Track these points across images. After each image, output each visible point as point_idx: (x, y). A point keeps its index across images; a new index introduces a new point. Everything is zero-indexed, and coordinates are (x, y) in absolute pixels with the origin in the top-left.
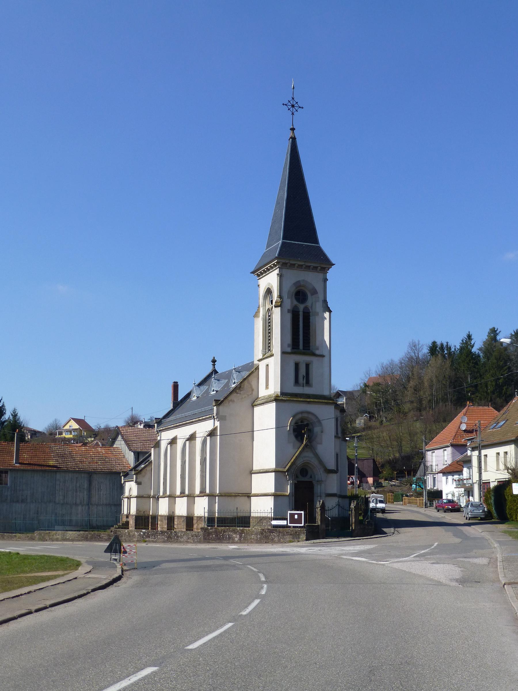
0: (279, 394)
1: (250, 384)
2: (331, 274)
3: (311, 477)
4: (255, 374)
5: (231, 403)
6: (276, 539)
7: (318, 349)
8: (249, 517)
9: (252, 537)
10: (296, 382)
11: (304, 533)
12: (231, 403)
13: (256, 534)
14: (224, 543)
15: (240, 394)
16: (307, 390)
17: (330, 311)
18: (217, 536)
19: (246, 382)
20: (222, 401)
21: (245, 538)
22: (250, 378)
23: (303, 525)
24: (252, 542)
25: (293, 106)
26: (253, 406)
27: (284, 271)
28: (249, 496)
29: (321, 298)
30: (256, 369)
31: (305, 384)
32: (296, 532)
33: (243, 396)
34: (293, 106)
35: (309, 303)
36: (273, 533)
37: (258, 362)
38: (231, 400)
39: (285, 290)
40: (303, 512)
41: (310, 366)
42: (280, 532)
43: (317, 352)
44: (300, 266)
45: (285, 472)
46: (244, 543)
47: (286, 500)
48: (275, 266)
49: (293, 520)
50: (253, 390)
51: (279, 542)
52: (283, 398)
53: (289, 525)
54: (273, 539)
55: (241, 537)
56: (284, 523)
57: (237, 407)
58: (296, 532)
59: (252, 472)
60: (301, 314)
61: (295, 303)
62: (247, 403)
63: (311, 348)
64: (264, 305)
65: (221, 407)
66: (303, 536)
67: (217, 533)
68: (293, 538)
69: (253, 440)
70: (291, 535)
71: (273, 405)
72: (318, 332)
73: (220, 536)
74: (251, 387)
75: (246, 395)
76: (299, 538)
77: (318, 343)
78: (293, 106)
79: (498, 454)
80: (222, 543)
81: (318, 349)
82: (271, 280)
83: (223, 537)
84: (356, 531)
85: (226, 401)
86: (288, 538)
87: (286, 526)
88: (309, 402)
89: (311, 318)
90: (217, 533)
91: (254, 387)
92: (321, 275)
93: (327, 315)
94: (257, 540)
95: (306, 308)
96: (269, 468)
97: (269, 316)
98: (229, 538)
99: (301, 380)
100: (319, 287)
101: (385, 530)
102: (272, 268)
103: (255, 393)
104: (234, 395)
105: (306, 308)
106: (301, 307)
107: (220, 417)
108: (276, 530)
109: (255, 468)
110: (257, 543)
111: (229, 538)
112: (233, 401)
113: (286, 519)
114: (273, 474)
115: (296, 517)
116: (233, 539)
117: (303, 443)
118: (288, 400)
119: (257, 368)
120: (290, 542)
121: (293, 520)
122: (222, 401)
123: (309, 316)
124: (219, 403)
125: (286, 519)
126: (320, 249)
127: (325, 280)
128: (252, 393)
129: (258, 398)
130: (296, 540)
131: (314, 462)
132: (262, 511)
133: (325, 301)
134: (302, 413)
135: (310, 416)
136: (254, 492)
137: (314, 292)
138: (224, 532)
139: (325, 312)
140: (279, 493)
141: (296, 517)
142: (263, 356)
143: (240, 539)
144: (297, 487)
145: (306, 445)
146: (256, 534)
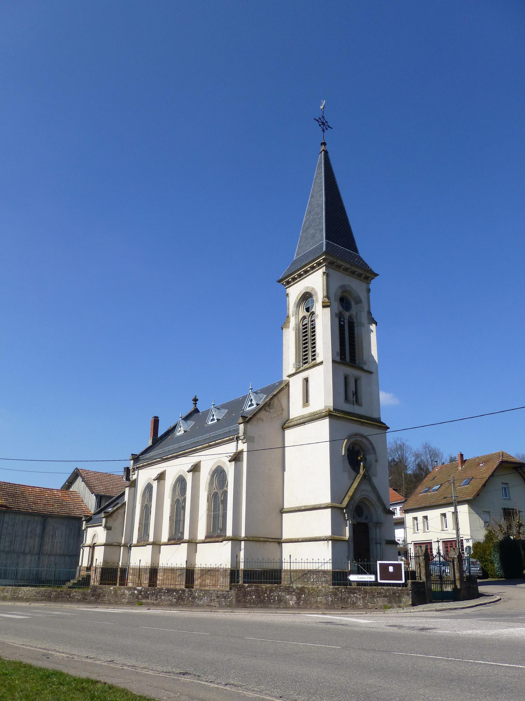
0: (332, 409)
1: (279, 401)
2: (374, 284)
3: (366, 518)
4: (285, 391)
5: (259, 421)
6: (360, 603)
7: (365, 364)
8: (280, 571)
9: (319, 599)
10: (346, 399)
11: (408, 594)
12: (259, 421)
13: (326, 595)
14: (270, 608)
15: (270, 412)
16: (357, 409)
17: (376, 324)
18: (258, 597)
19: (275, 399)
20: (251, 419)
21: (306, 601)
22: (279, 395)
23: (403, 581)
24: (318, 608)
25: (323, 124)
26: (284, 428)
27: (331, 271)
28: (279, 542)
29: (366, 309)
30: (286, 385)
31: (355, 402)
32: (394, 593)
33: (273, 416)
34: (323, 124)
35: (354, 311)
36: (354, 593)
37: (287, 378)
38: (260, 419)
39: (332, 291)
40: (379, 562)
41: (359, 382)
42: (366, 593)
43: (365, 367)
44: (346, 270)
45: (343, 509)
46: (305, 608)
47: (345, 546)
48: (319, 264)
49: (385, 574)
50: (283, 410)
51: (365, 607)
52: (337, 414)
53: (379, 581)
54: (354, 603)
55: (299, 599)
56: (371, 578)
57: (266, 427)
58: (394, 593)
59: (282, 511)
60: (346, 322)
61: (341, 309)
62: (278, 425)
63: (357, 362)
64: (297, 313)
65: (249, 426)
66: (407, 599)
67: (258, 593)
68: (390, 602)
69: (284, 469)
70: (385, 596)
71: (327, 421)
72: (365, 345)
73: (264, 597)
74: (281, 406)
75: (276, 415)
76: (400, 602)
77: (365, 358)
78: (323, 124)
79: (444, 515)
80: (267, 607)
81: (365, 364)
82: (316, 281)
83: (269, 600)
84: (462, 591)
85: (255, 418)
86: (380, 601)
87: (375, 584)
88: (363, 423)
89: (356, 329)
90: (258, 593)
91: (284, 406)
92: (364, 285)
93: (373, 327)
94: (326, 604)
95: (350, 317)
96: (309, 504)
97: (312, 321)
98: (280, 600)
99: (350, 395)
100: (363, 296)
101: (482, 589)
102: (313, 268)
103: (285, 413)
104: (263, 412)
105: (350, 317)
106: (347, 314)
107: (248, 439)
108: (360, 590)
109: (287, 505)
110: (326, 608)
111: (280, 600)
112: (262, 420)
113: (375, 573)
114: (328, 512)
115: (391, 569)
116: (286, 602)
117: (358, 472)
118: (341, 417)
119: (288, 385)
120: (386, 608)
121: (385, 574)
122: (251, 419)
123: (354, 327)
124: (247, 420)
125: (375, 573)
126: (360, 259)
127: (369, 290)
128: (282, 414)
129: (288, 419)
130: (395, 605)
131: (373, 497)
132: (316, 560)
133: (369, 313)
134: (356, 435)
135: (364, 440)
136: (285, 536)
137: (359, 301)
138: (271, 591)
139: (371, 324)
140: (337, 537)
141: (391, 569)
142: (297, 370)
143: (298, 603)
144: (356, 529)
145: (364, 476)
146: (326, 595)
